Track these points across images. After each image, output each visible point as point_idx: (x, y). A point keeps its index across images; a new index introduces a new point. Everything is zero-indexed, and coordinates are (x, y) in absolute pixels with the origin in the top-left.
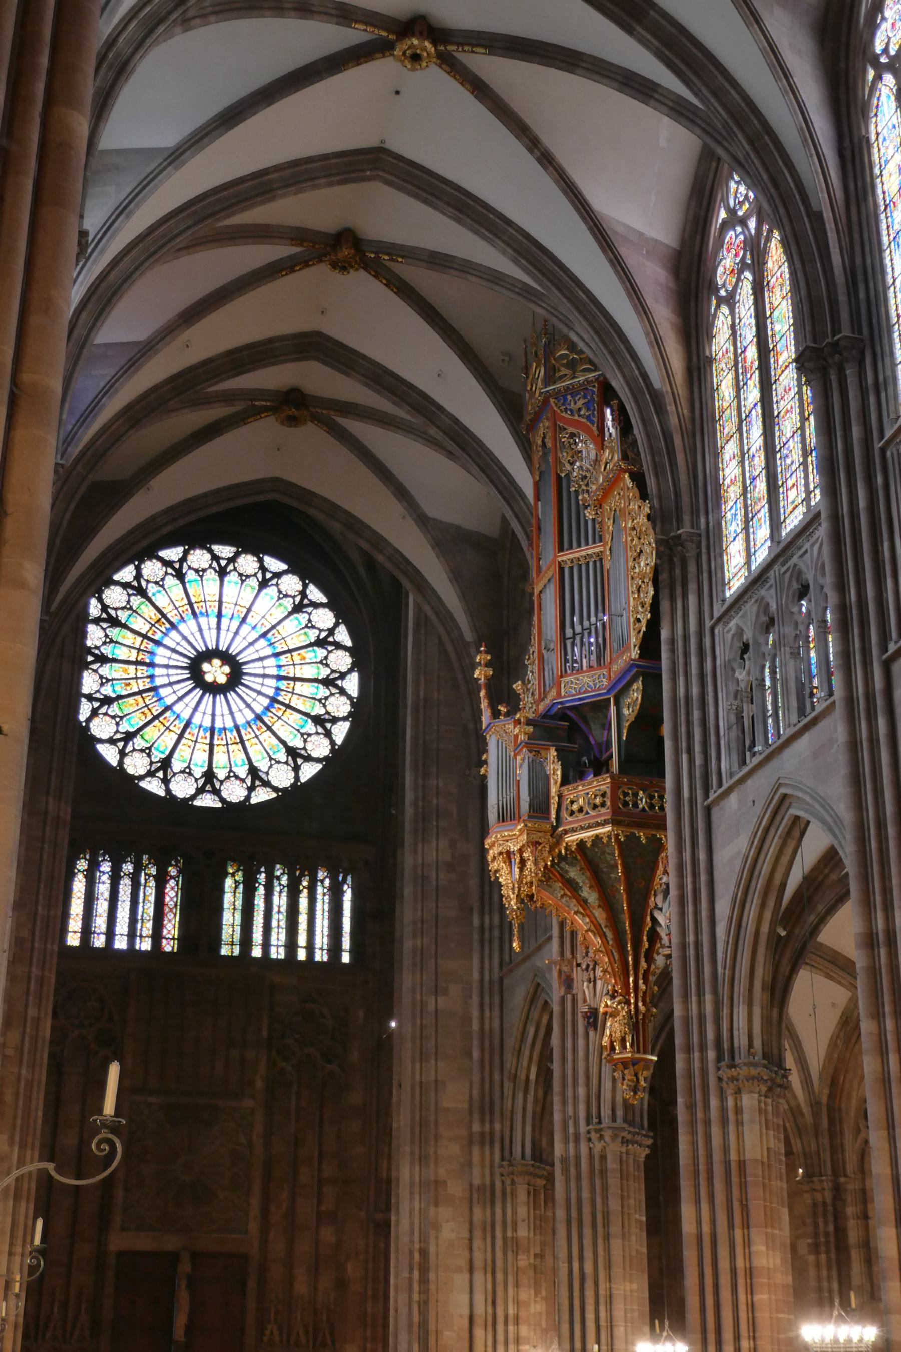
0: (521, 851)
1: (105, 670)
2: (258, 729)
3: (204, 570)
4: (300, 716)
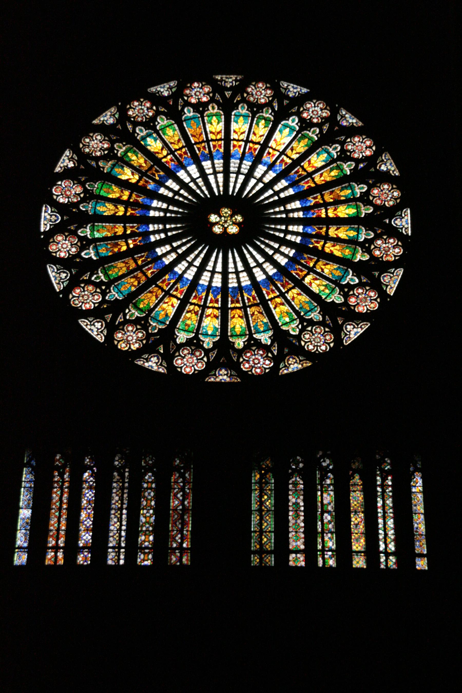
1: (86, 232)
2: (283, 286)
3: (205, 105)
4: (336, 266)
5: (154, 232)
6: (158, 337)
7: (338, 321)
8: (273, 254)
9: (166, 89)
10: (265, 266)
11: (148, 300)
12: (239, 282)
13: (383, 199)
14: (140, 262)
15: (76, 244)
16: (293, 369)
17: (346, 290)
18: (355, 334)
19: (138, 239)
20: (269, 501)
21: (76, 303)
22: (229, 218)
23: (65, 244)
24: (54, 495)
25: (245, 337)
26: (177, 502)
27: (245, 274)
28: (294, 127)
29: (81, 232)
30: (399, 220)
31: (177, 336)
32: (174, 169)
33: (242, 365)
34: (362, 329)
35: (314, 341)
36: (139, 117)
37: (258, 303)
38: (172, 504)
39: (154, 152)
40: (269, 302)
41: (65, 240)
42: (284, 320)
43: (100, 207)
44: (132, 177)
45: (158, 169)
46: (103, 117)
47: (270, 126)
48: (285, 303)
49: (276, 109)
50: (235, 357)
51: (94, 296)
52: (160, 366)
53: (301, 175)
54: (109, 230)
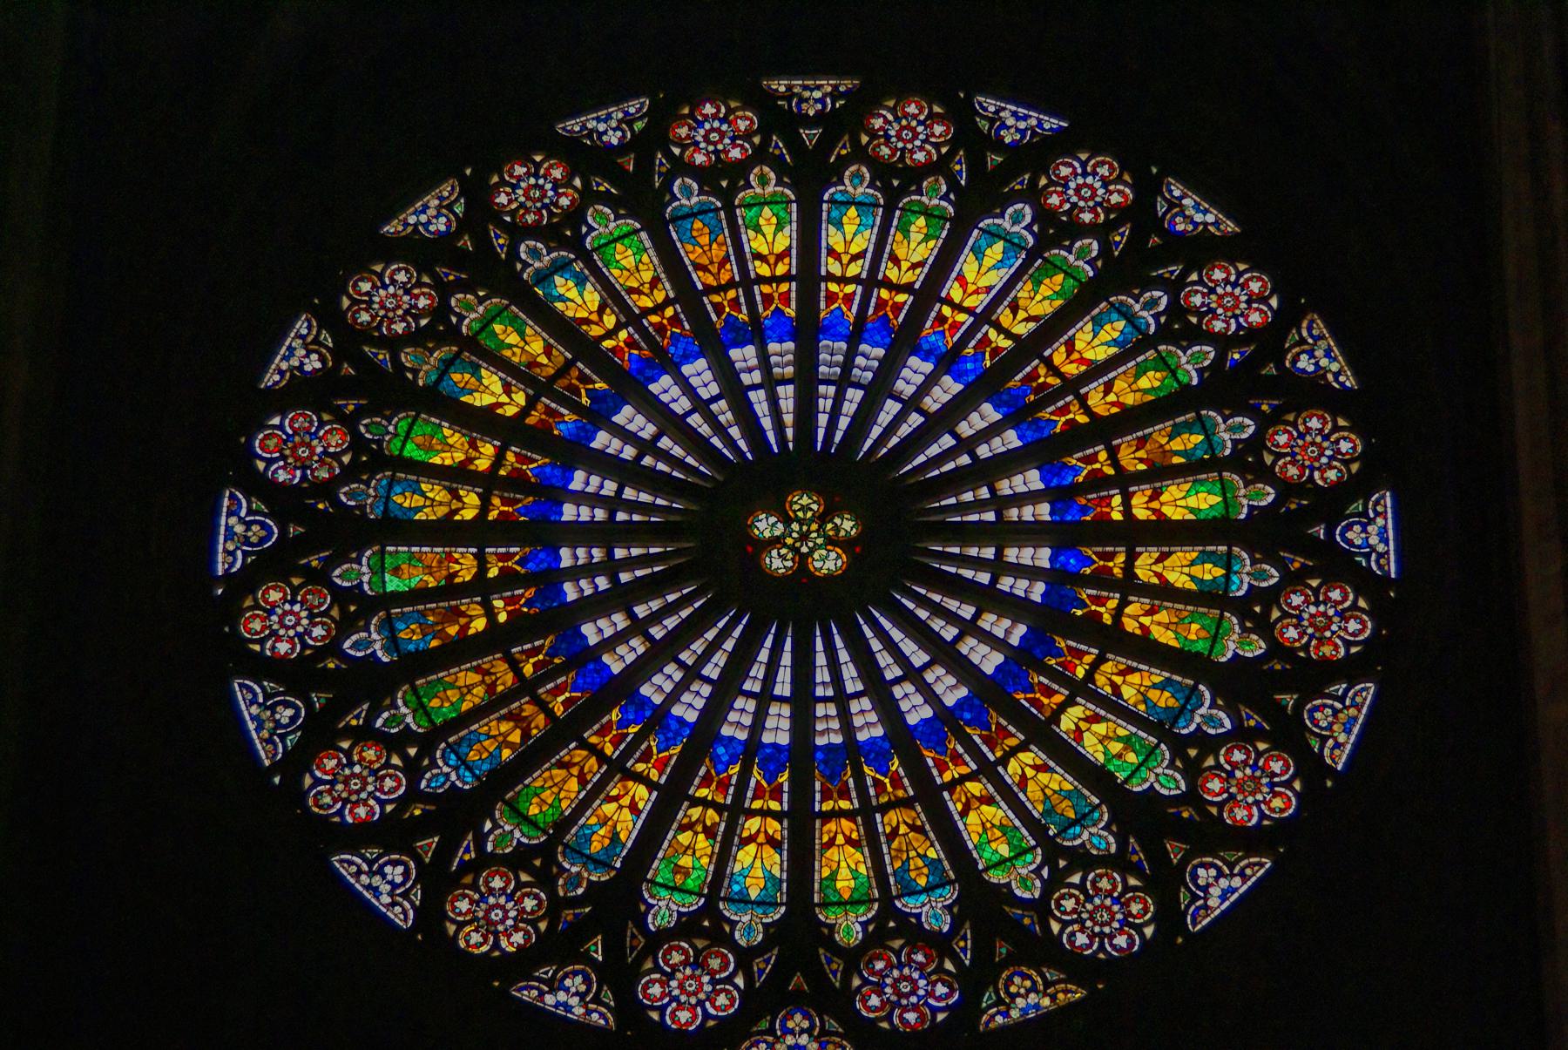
1: (357, 573)
5: (575, 573)
6: (587, 910)
7: (1168, 853)
8: (958, 638)
9: (614, 124)
10: (929, 677)
11: (555, 789)
12: (848, 728)
13: (1307, 463)
14: (528, 669)
15: (325, 614)
16: (1024, 1011)
17: (1193, 753)
18: (1223, 898)
19: (522, 596)
21: (323, 802)
22: (814, 527)
23: (291, 612)
25: (870, 909)
27: (866, 703)
28: (1021, 237)
29: (339, 576)
30: (1357, 528)
32: (640, 371)
34: (1244, 878)
35: (1092, 919)
36: (528, 211)
37: (910, 798)
39: (574, 319)
40: (946, 794)
41: (293, 602)
43: (403, 494)
44: (504, 399)
45: (587, 371)
46: (414, 213)
47: (944, 234)
48: (998, 798)
49: (963, 182)
50: (834, 973)
51: (383, 778)
52: (591, 1006)
53: (1045, 385)
54: (431, 567)
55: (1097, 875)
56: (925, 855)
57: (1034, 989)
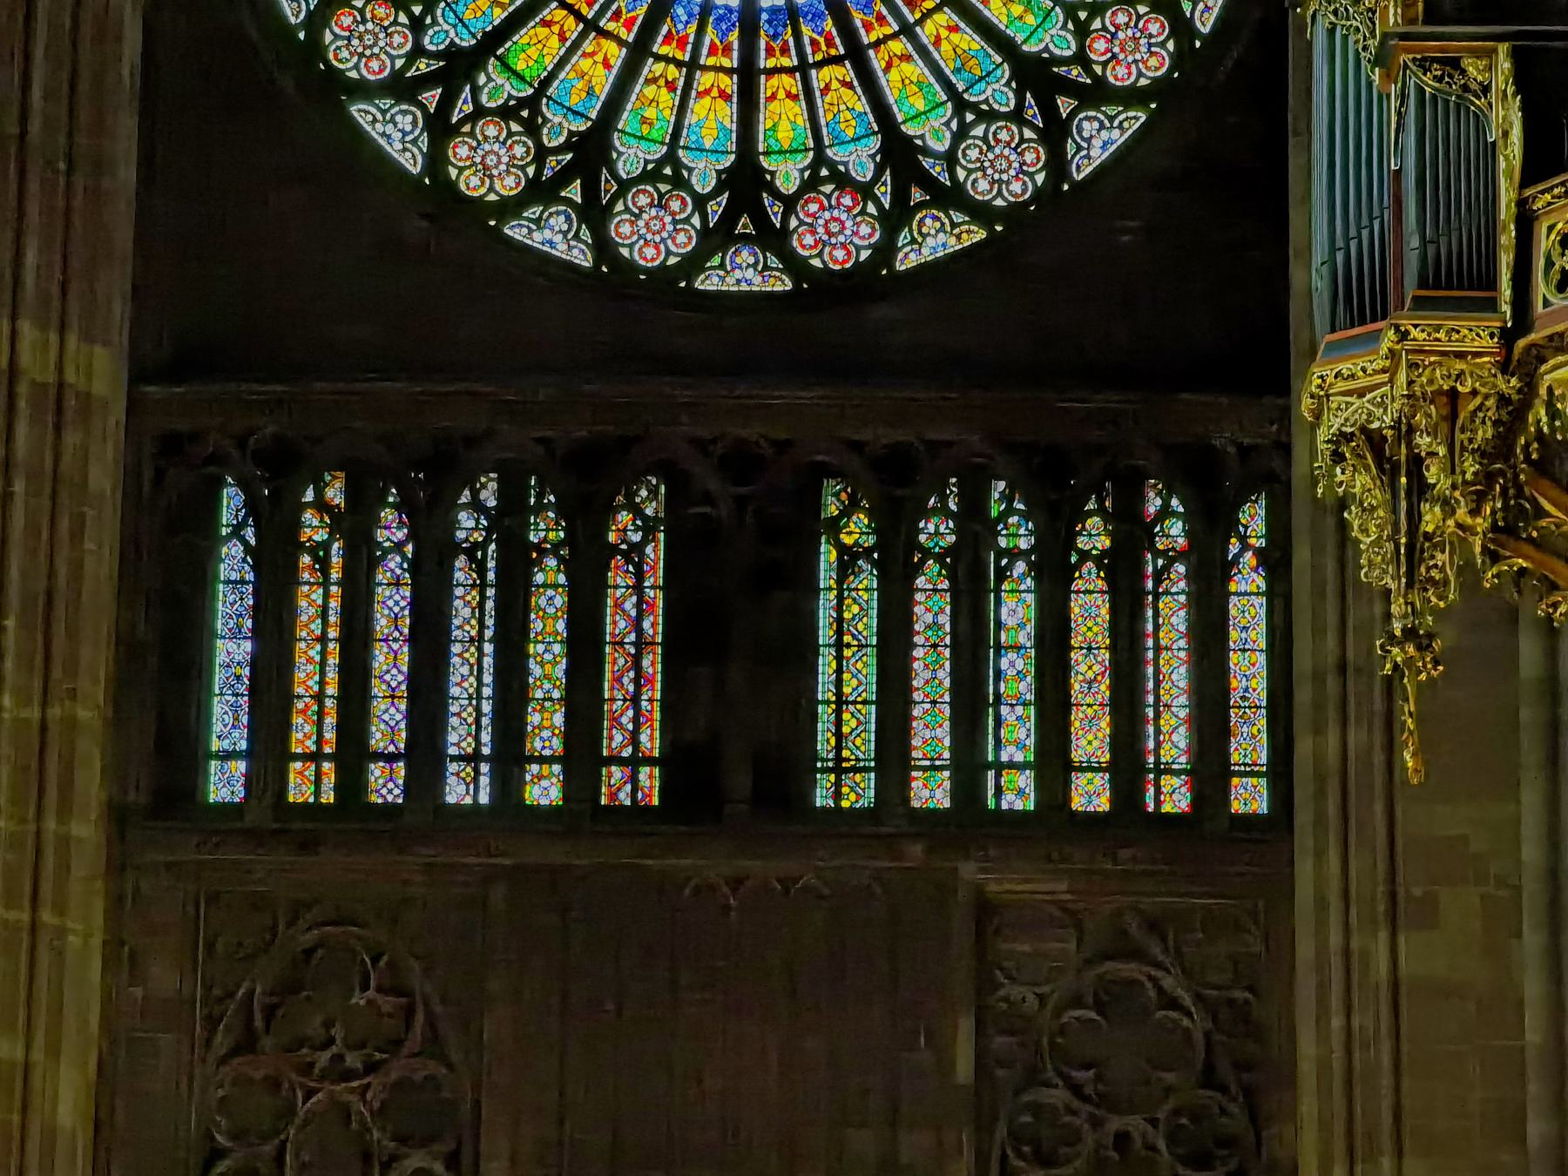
0: (1406, 430)
6: (569, 156)
11: (540, 46)
20: (865, 619)
24: (303, 603)
26: (622, 624)
31: (620, 154)
33: (795, 236)
35: (992, 166)
38: (608, 629)
40: (871, 52)
42: (912, 106)
48: (916, 56)
50: (775, 214)
55: (998, 128)
56: (853, 109)
57: (942, 229)
